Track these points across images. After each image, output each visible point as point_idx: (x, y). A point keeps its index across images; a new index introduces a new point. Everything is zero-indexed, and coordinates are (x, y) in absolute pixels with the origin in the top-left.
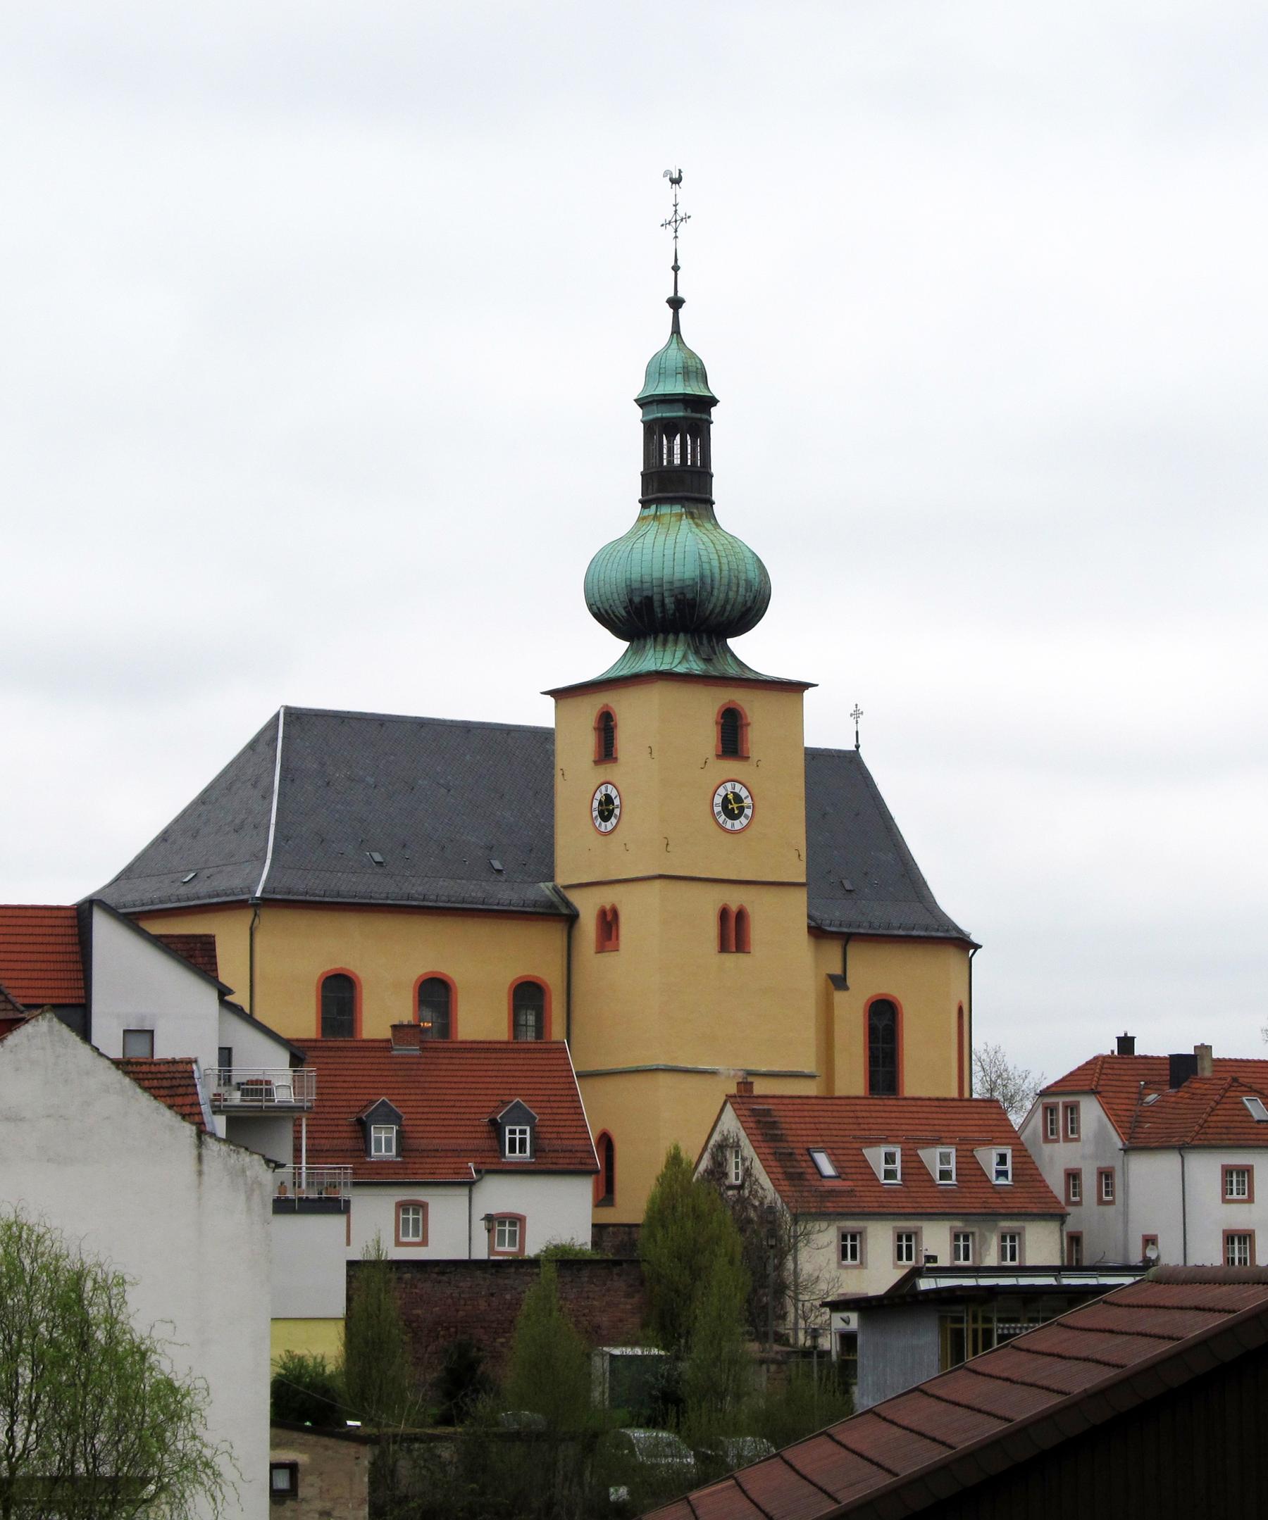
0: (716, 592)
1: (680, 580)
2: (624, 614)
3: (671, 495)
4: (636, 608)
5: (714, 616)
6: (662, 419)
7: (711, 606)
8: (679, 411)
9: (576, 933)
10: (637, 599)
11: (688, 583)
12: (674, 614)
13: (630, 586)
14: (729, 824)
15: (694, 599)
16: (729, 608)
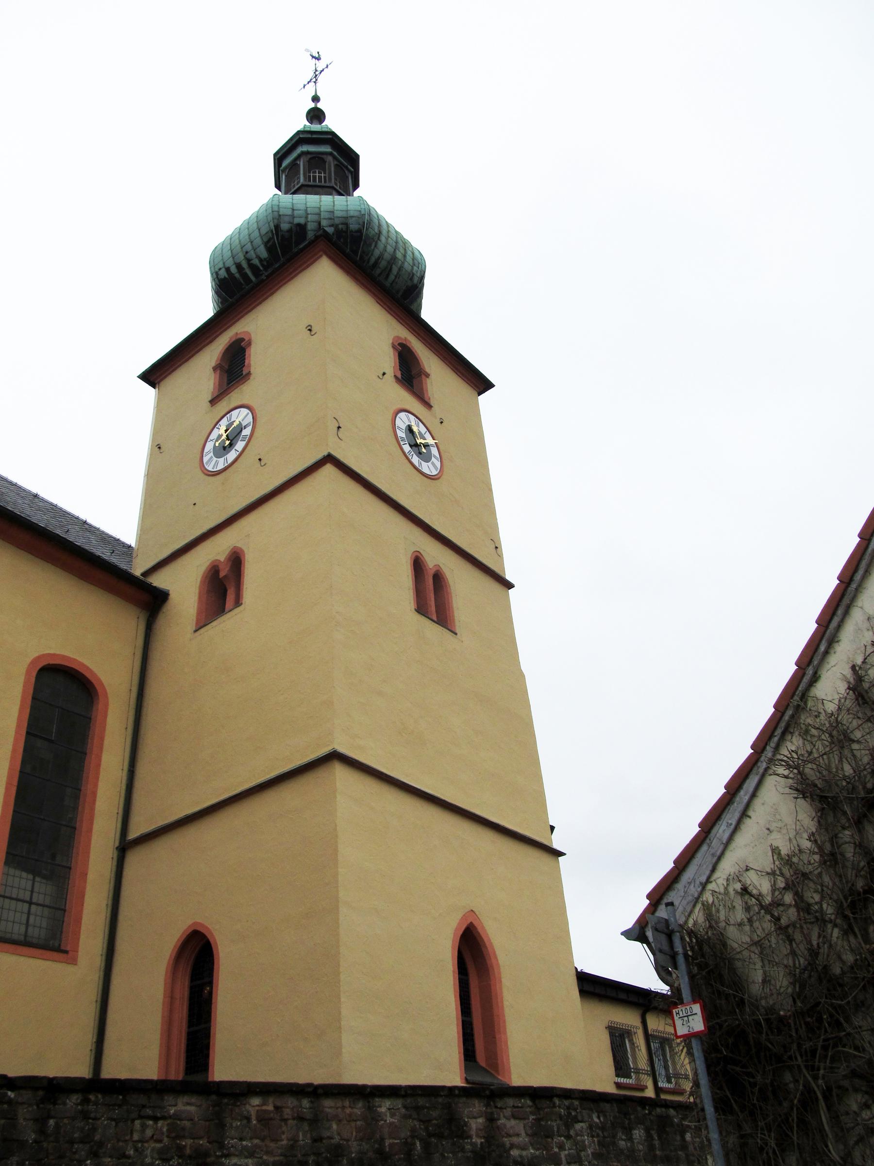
0: (383, 239)
2: (264, 254)
4: (282, 236)
5: (378, 271)
6: (308, 153)
7: (377, 253)
9: (162, 621)
10: (285, 226)
11: (352, 214)
13: (278, 212)
14: (415, 460)
15: (360, 231)
16: (395, 270)
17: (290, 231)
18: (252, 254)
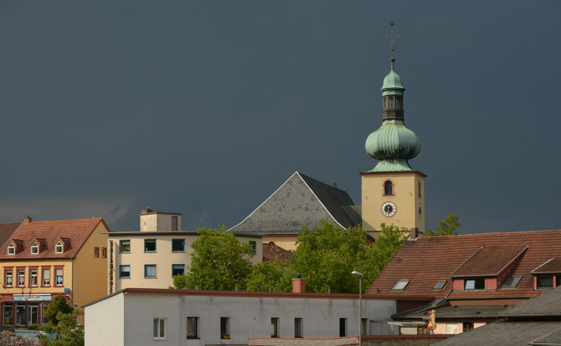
1: (412, 144)
2: (394, 152)
3: (399, 118)
8: (400, 93)
10: (401, 148)
11: (414, 145)
12: (407, 154)
17: (401, 149)
18: (391, 150)
